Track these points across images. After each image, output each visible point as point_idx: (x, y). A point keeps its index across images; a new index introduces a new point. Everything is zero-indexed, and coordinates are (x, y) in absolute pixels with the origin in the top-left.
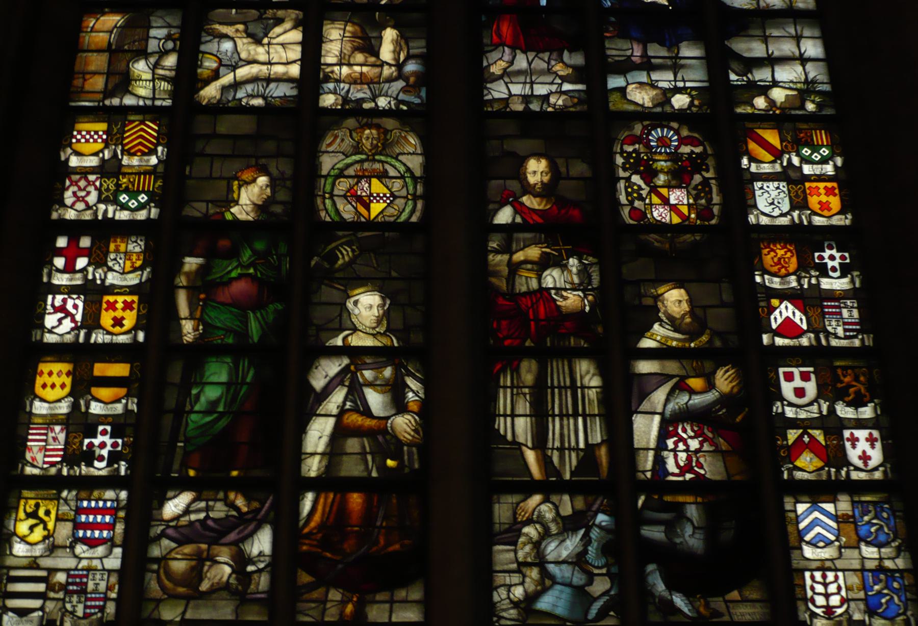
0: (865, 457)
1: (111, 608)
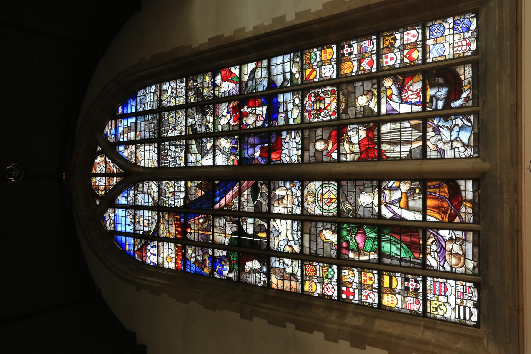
0: (414, 36)
1: (469, 284)
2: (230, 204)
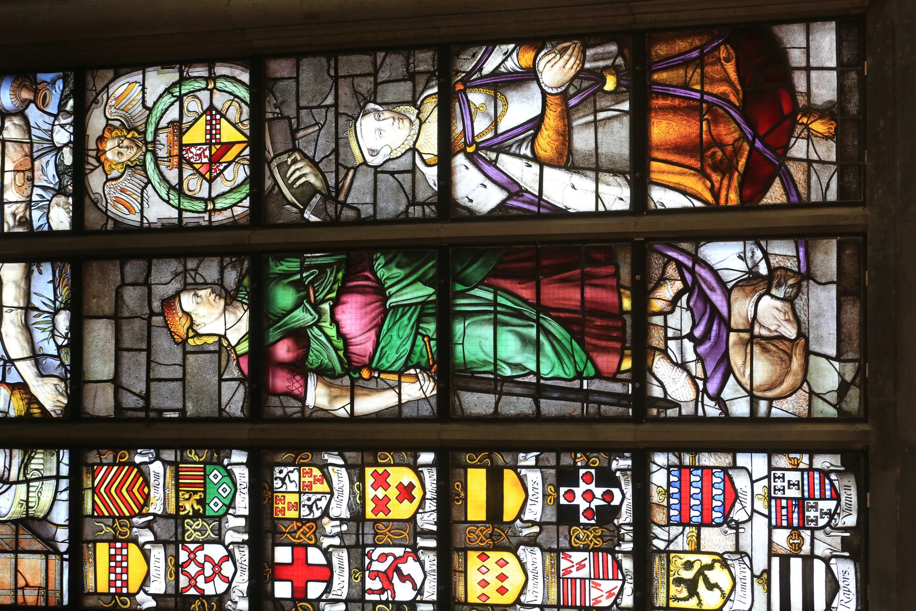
1: (822, 462)
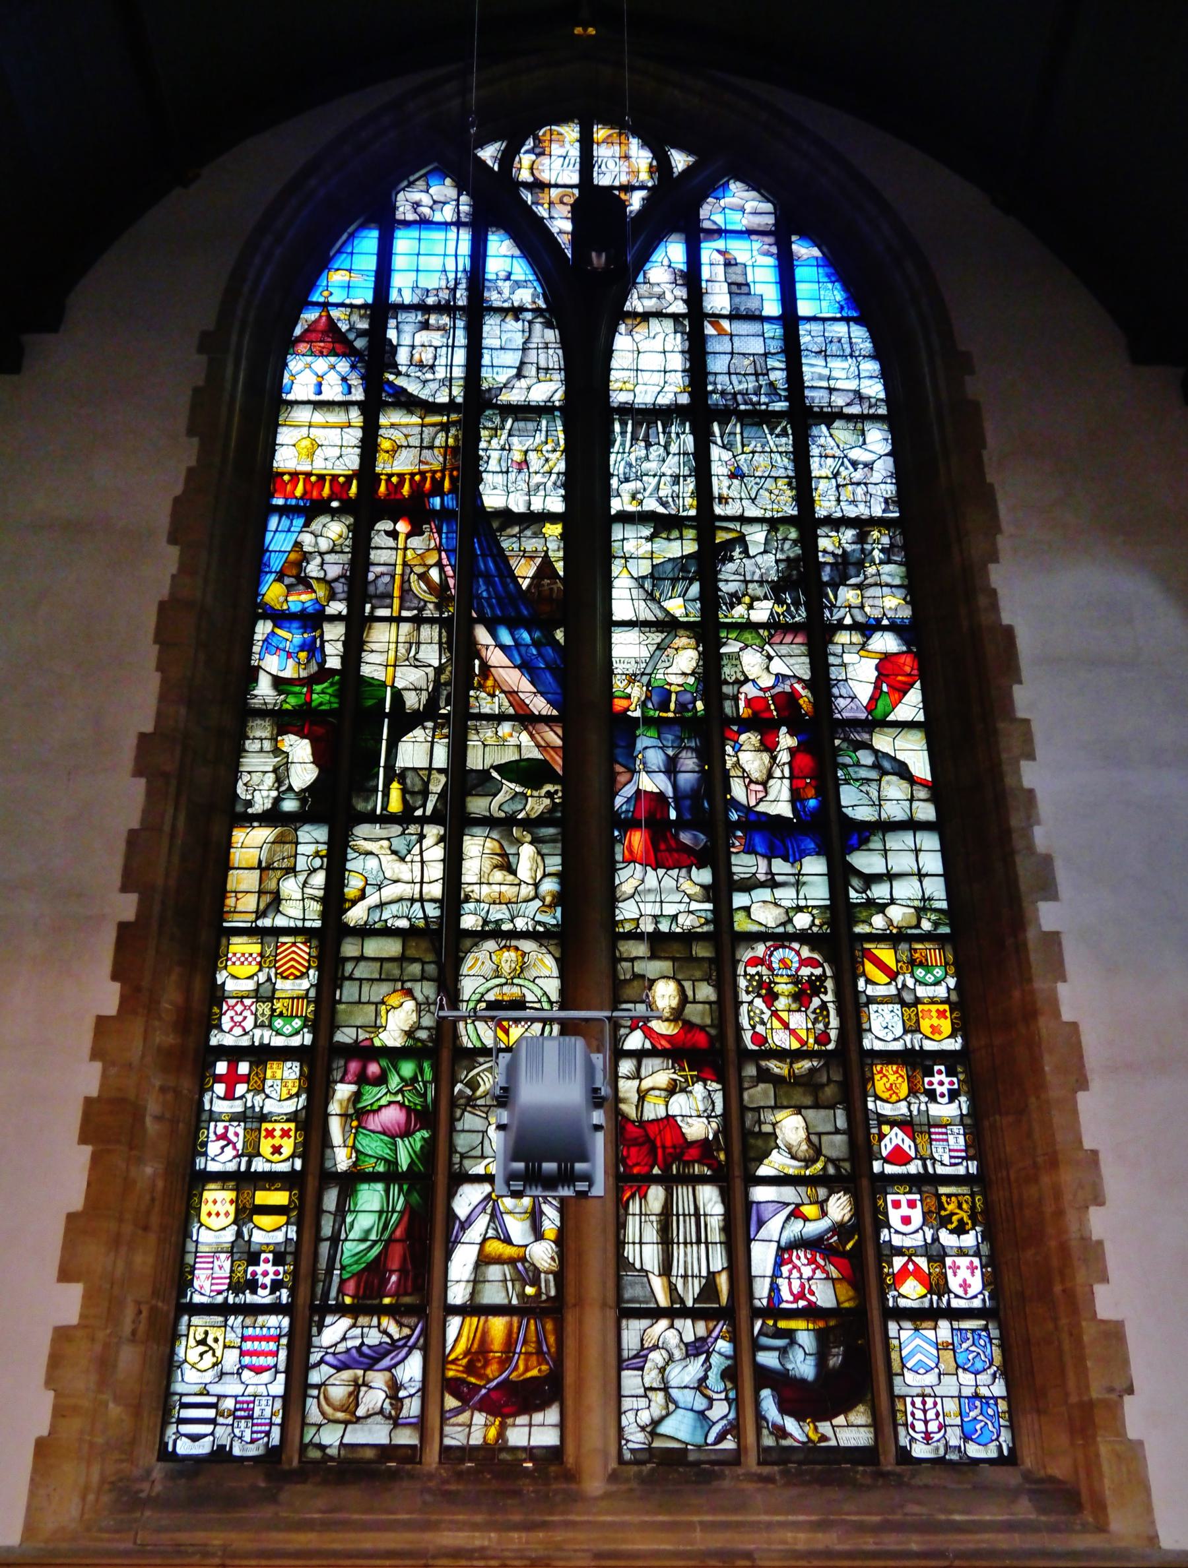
0: (965, 1285)
1: (276, 1433)
2: (490, 683)
